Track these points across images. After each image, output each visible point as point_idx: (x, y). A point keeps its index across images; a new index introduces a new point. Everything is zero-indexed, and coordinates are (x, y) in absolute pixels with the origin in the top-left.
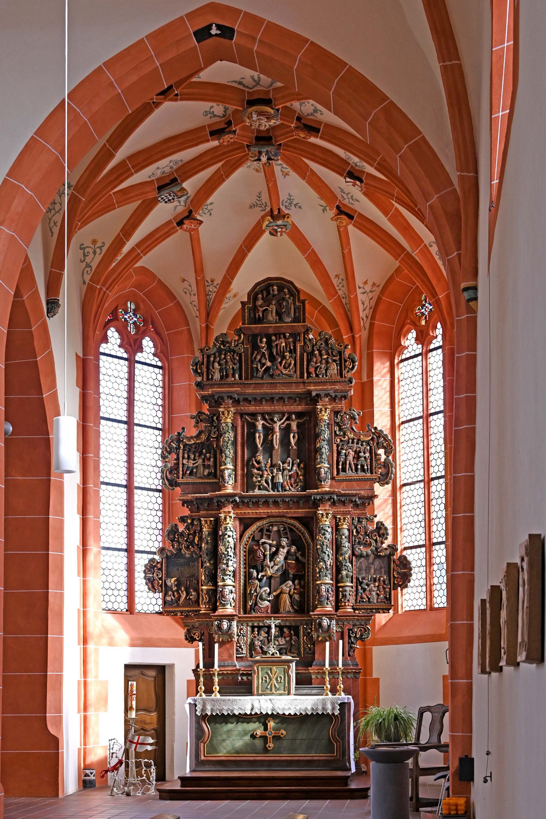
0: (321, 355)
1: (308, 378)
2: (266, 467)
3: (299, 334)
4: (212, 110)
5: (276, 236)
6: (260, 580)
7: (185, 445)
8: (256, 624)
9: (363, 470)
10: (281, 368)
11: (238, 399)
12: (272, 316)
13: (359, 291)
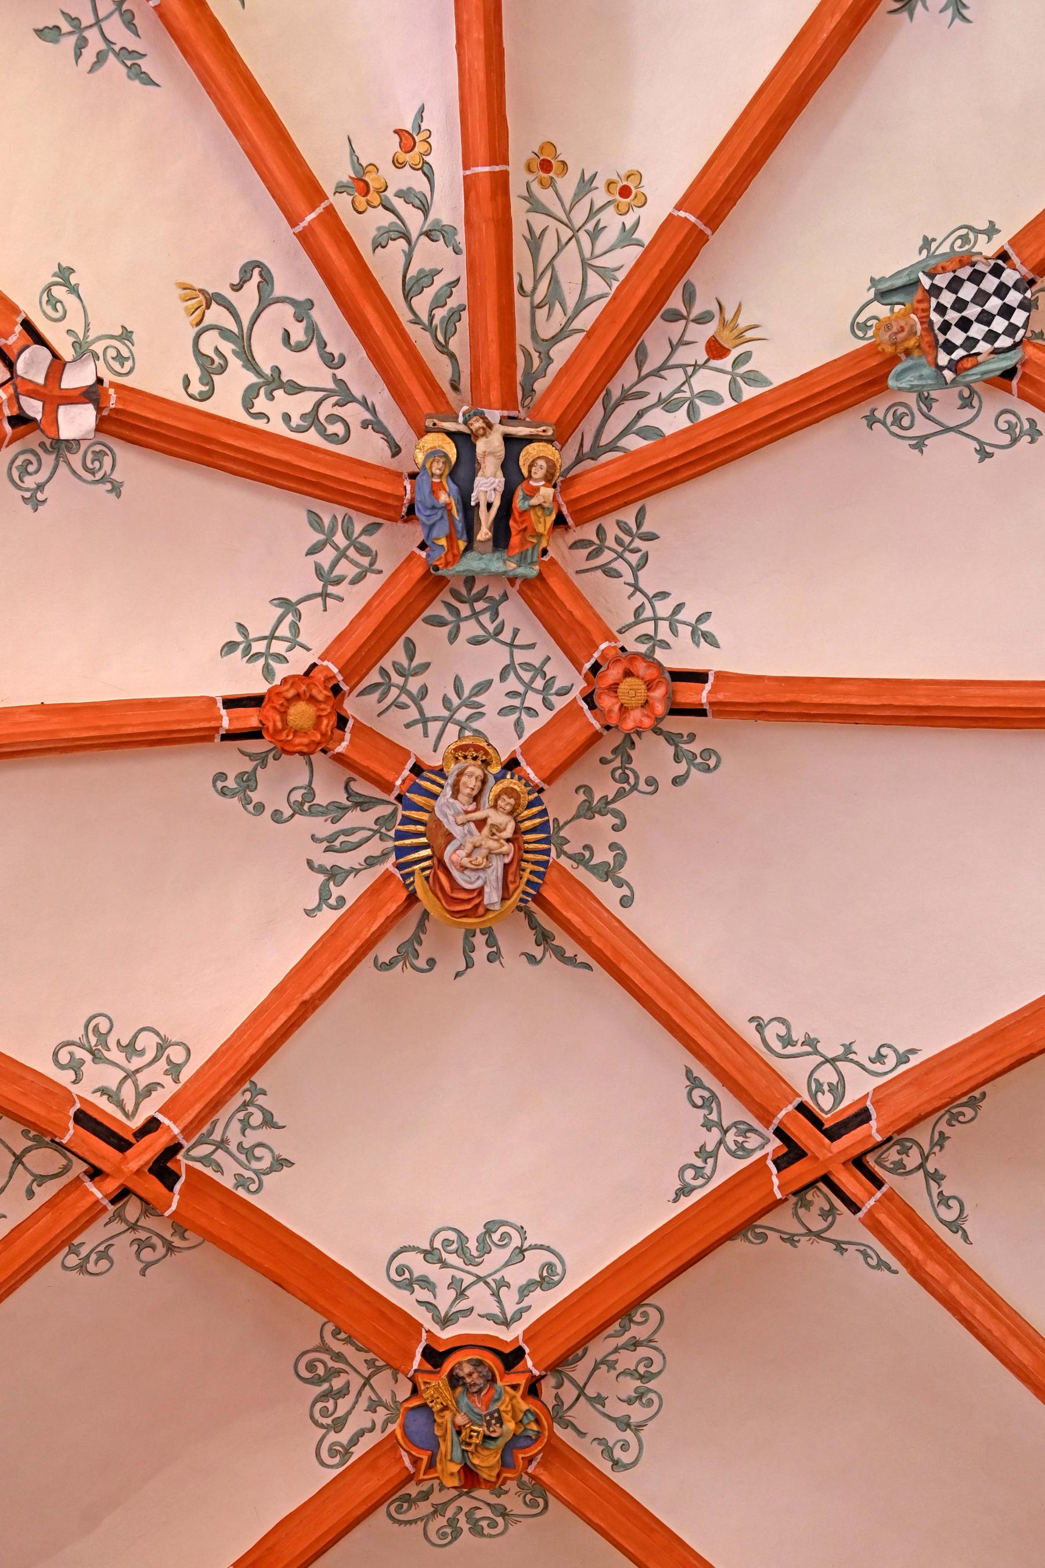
4: (682, 768)
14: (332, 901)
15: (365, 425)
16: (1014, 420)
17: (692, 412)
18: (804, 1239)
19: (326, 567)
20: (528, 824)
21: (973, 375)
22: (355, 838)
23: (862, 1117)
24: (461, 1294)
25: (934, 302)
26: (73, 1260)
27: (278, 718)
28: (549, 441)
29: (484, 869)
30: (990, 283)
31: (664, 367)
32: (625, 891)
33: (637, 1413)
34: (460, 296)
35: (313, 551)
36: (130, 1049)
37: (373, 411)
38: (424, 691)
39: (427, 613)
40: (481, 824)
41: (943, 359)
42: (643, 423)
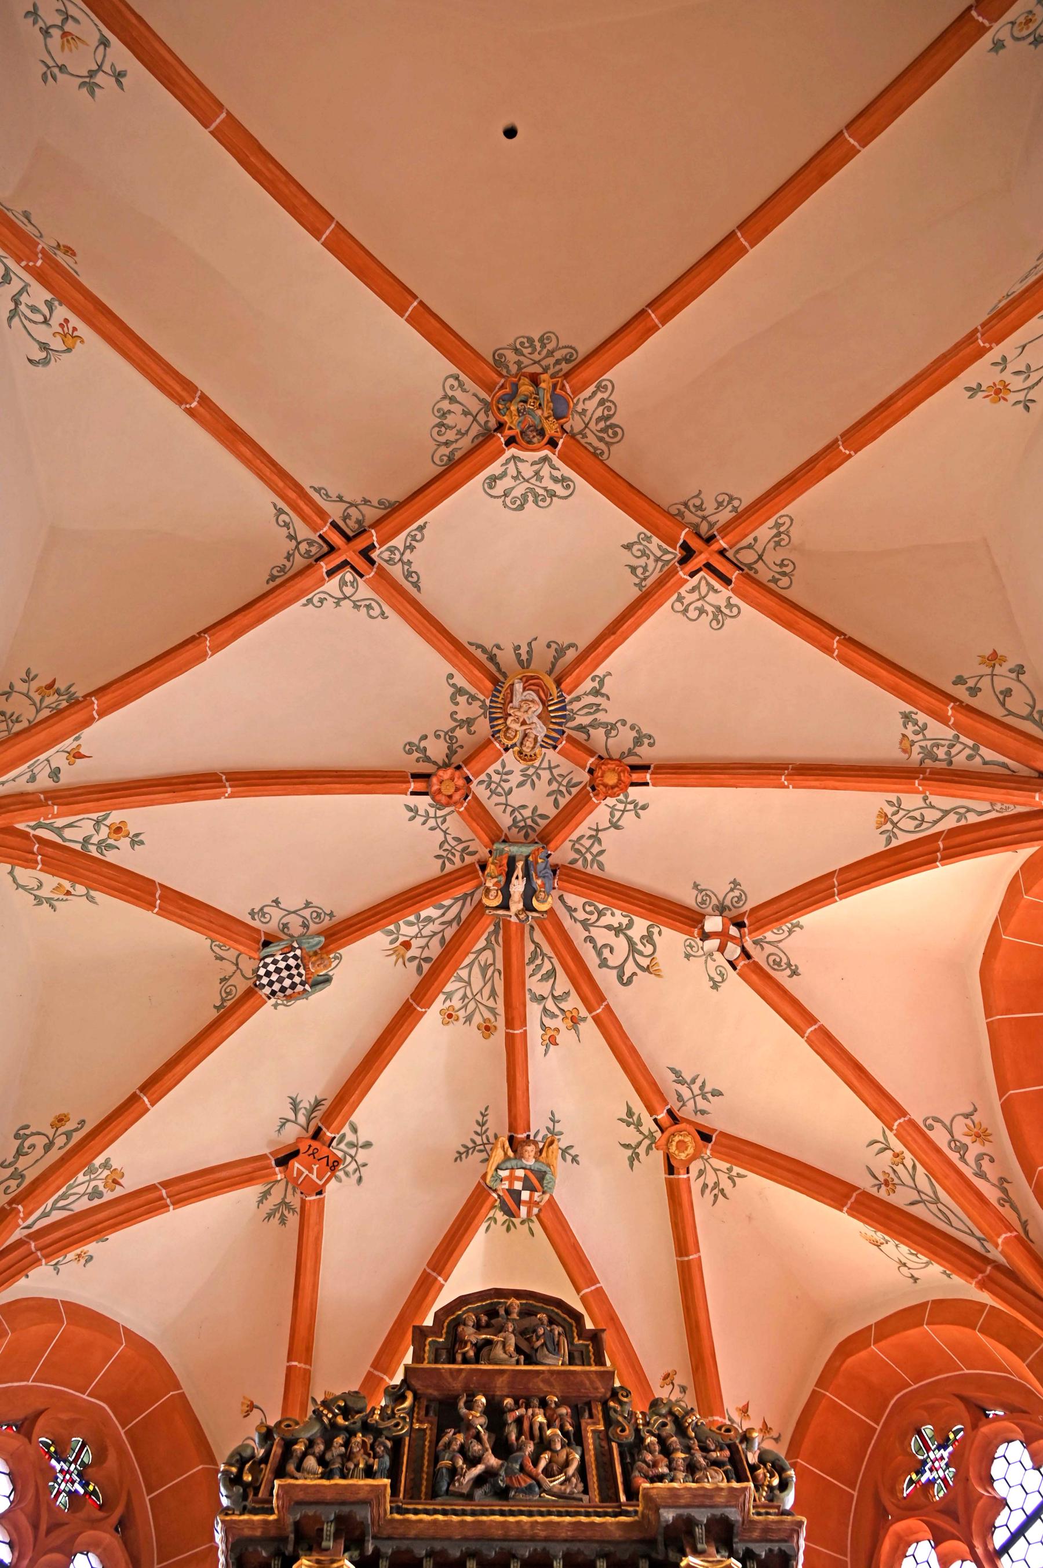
4: (423, 744)
14: (598, 679)
15: (575, 910)
16: (262, 919)
17: (418, 917)
18: (359, 502)
19: (596, 844)
20: (500, 721)
21: (283, 945)
22: (586, 710)
23: (331, 573)
24: (537, 473)
25: (304, 978)
26: (736, 503)
27: (623, 778)
28: (488, 907)
29: (523, 701)
30: (276, 987)
31: (432, 937)
32: (451, 682)
33: (445, 405)
34: (529, 970)
35: (602, 852)
36: (702, 611)
37: (571, 916)
38: (550, 782)
39: (548, 821)
40: (524, 723)
41: (298, 952)
42: (442, 911)
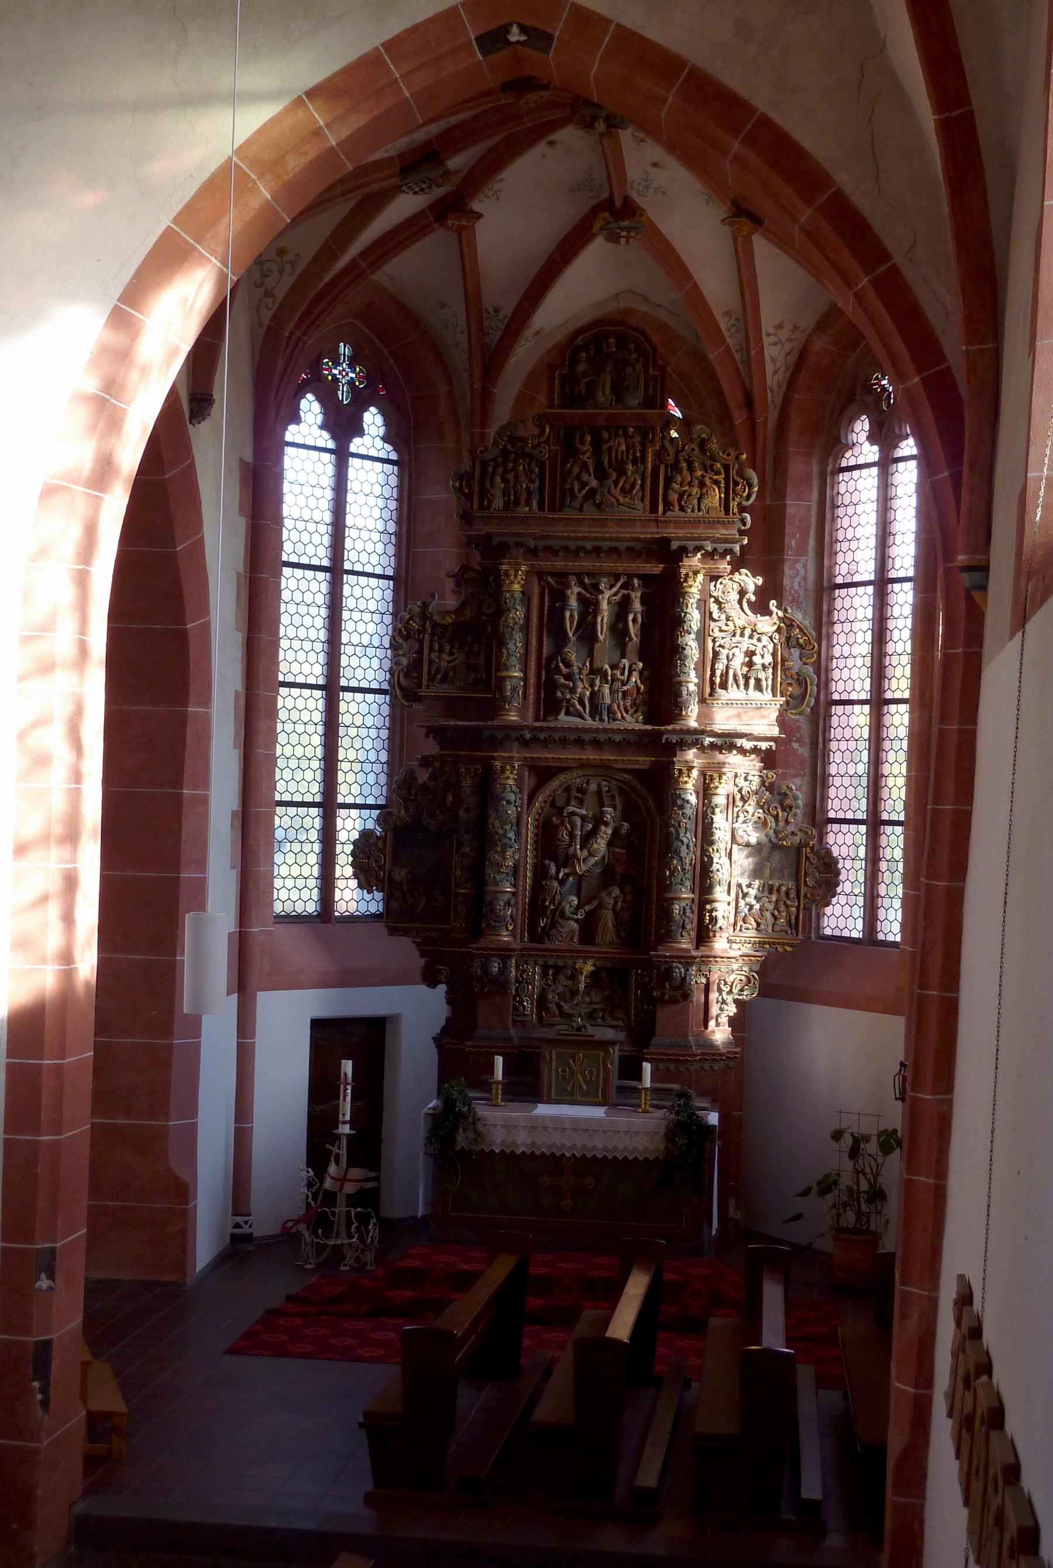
0: (691, 470)
1: (664, 512)
2: (580, 673)
3: (653, 429)
5: (618, 243)
6: (562, 882)
7: (435, 625)
8: (551, 962)
9: (758, 687)
10: (616, 492)
11: (535, 546)
12: (604, 394)
13: (766, 341)
